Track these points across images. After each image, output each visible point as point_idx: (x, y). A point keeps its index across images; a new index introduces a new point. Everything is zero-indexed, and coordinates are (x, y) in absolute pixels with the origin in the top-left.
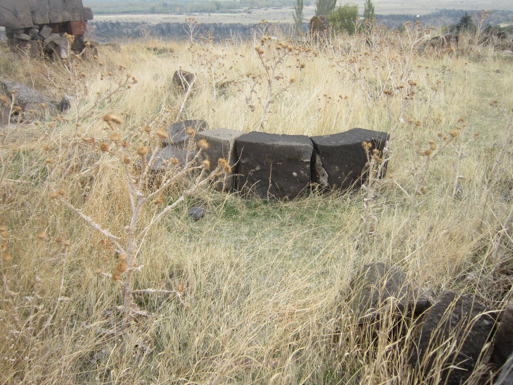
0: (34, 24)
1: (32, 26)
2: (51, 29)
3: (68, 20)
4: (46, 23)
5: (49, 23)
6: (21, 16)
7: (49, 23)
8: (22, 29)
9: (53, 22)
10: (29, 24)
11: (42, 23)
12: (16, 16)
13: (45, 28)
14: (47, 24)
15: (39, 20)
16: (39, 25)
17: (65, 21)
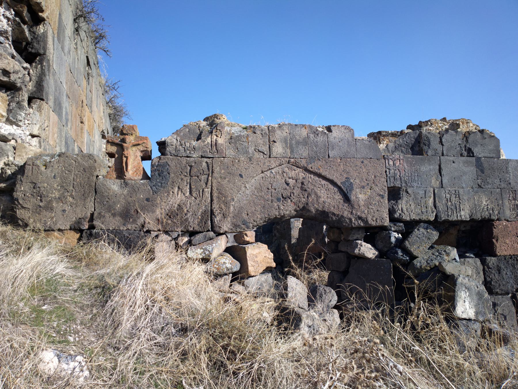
0: (393, 220)
1: (387, 222)
2: (435, 235)
3: (486, 215)
4: (424, 218)
5: (432, 218)
6: (360, 196)
7: (432, 218)
8: (359, 228)
9: (443, 217)
10: (379, 216)
11: (414, 217)
12: (347, 199)
13: (420, 232)
14: (428, 222)
15: (407, 209)
16: (406, 223)
17: (478, 216)
